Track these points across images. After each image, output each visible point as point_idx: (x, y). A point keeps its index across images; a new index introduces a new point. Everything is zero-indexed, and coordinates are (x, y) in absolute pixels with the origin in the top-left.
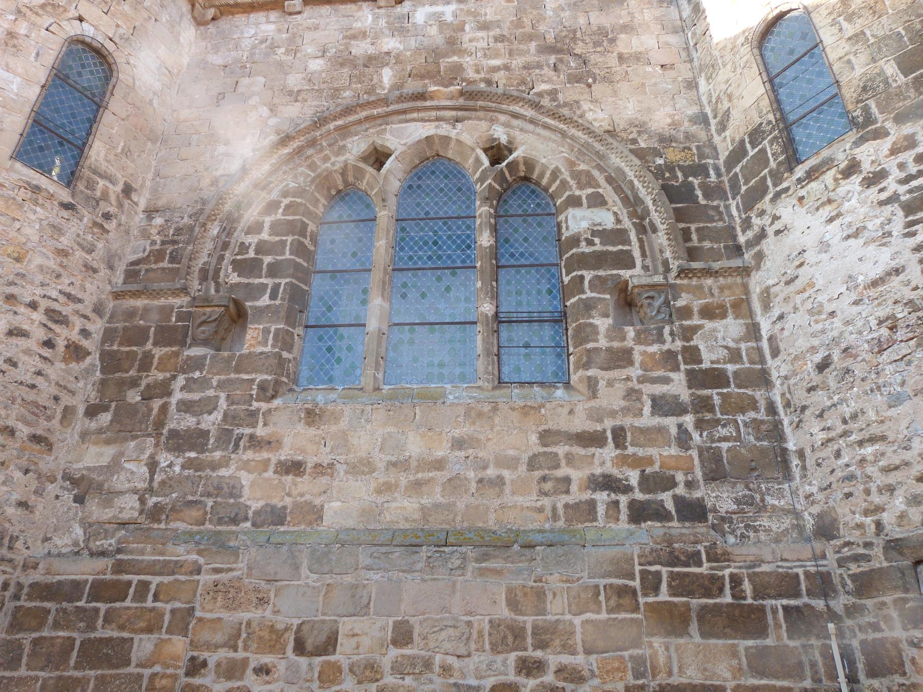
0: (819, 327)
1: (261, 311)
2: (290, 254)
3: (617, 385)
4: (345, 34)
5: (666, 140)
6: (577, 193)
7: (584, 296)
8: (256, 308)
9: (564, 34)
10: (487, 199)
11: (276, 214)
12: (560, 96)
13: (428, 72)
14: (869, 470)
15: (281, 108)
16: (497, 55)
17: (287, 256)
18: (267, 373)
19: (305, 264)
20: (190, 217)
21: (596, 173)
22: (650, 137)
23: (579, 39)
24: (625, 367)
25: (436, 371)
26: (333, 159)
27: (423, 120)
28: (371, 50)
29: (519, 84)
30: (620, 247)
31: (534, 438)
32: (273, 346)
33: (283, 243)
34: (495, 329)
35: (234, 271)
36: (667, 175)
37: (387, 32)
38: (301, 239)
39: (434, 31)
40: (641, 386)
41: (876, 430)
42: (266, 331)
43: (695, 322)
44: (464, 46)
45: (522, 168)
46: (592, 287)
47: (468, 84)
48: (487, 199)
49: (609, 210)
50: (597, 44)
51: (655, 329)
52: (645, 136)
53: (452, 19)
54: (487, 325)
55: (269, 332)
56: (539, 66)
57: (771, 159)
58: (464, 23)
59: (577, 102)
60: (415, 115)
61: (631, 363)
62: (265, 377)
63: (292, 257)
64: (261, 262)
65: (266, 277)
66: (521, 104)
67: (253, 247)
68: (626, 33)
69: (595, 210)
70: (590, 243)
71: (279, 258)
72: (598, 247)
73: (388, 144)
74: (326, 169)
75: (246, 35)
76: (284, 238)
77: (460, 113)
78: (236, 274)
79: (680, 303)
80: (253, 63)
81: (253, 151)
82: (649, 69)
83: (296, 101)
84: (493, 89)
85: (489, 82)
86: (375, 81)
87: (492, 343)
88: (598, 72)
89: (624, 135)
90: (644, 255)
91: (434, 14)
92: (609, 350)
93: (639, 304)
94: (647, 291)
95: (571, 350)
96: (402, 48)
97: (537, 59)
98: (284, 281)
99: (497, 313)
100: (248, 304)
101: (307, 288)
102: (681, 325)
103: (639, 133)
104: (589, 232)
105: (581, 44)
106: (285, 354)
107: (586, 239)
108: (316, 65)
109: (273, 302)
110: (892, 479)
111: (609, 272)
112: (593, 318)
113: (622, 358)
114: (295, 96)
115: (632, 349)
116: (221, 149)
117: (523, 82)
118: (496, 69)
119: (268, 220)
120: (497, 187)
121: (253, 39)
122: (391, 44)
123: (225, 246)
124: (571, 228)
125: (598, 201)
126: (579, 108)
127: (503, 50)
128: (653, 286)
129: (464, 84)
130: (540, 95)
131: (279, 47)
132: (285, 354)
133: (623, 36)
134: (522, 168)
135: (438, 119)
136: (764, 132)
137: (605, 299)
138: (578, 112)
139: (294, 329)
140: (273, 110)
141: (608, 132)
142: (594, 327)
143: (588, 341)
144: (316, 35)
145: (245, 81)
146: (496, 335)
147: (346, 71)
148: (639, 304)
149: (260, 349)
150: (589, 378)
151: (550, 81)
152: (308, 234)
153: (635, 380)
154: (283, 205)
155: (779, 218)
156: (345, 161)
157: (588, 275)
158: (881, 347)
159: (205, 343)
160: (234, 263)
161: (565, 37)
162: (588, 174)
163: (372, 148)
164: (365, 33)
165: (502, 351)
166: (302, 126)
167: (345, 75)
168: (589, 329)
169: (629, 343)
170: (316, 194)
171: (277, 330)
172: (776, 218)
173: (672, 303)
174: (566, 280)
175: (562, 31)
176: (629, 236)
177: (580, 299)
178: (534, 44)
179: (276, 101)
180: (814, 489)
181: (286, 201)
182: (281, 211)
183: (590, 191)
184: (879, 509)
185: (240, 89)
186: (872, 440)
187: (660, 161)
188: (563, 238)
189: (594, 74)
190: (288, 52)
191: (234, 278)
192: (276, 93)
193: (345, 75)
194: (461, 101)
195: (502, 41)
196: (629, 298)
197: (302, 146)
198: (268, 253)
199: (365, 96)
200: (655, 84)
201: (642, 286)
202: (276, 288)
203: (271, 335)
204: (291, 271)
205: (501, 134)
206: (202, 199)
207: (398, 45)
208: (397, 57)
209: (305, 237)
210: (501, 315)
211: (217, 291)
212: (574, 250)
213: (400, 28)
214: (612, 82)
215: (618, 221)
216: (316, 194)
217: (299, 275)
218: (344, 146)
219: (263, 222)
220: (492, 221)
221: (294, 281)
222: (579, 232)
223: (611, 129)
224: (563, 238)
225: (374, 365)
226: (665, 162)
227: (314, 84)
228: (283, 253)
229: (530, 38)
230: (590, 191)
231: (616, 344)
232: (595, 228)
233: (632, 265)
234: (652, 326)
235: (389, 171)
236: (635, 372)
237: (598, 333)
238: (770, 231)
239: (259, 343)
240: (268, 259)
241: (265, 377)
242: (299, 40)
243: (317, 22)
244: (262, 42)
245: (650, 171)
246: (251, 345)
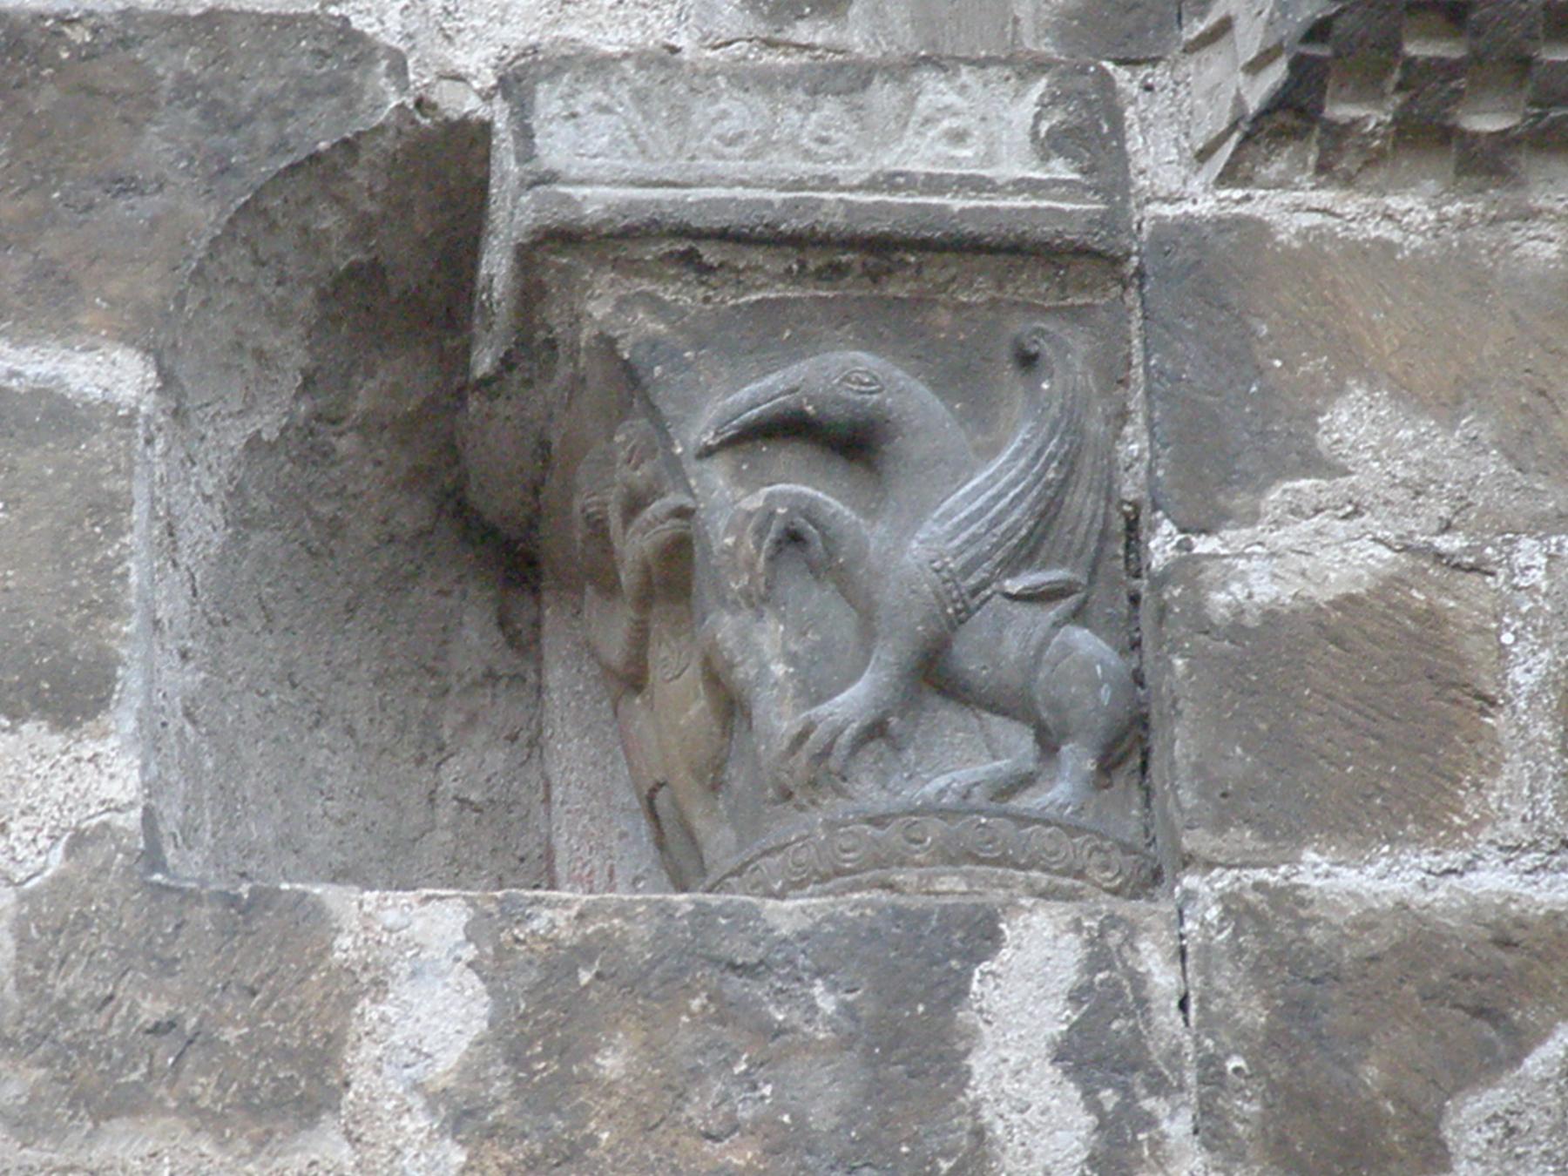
43: (1493, 880)
79: (1279, 558)
93: (635, 546)
102: (1267, 922)
128: (874, 262)
137: (58, 415)
148: (635, 546)
173: (1162, 544)
196: (494, 440)
201: (691, 246)
234: (787, 914)
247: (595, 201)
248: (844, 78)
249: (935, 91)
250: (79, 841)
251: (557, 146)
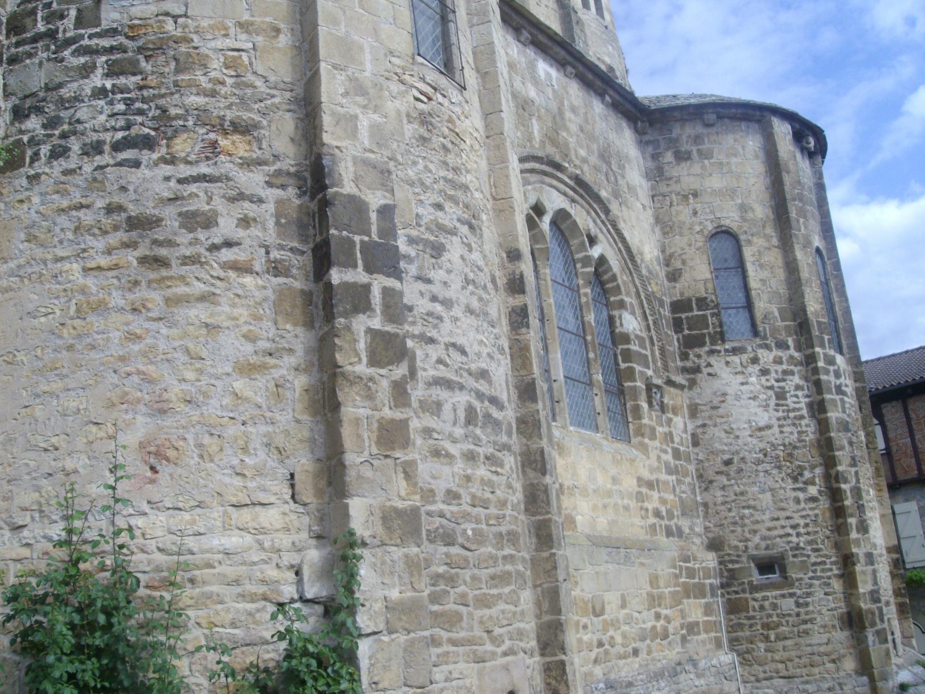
0: (729, 441)
14: (746, 521)
31: (635, 481)
41: (752, 503)
57: (711, 326)
60: (555, 183)
110: (756, 527)
136: (708, 305)
155: (711, 366)
158: (758, 462)
172: (709, 365)
180: (711, 525)
184: (747, 540)
186: (749, 507)
238: (705, 371)
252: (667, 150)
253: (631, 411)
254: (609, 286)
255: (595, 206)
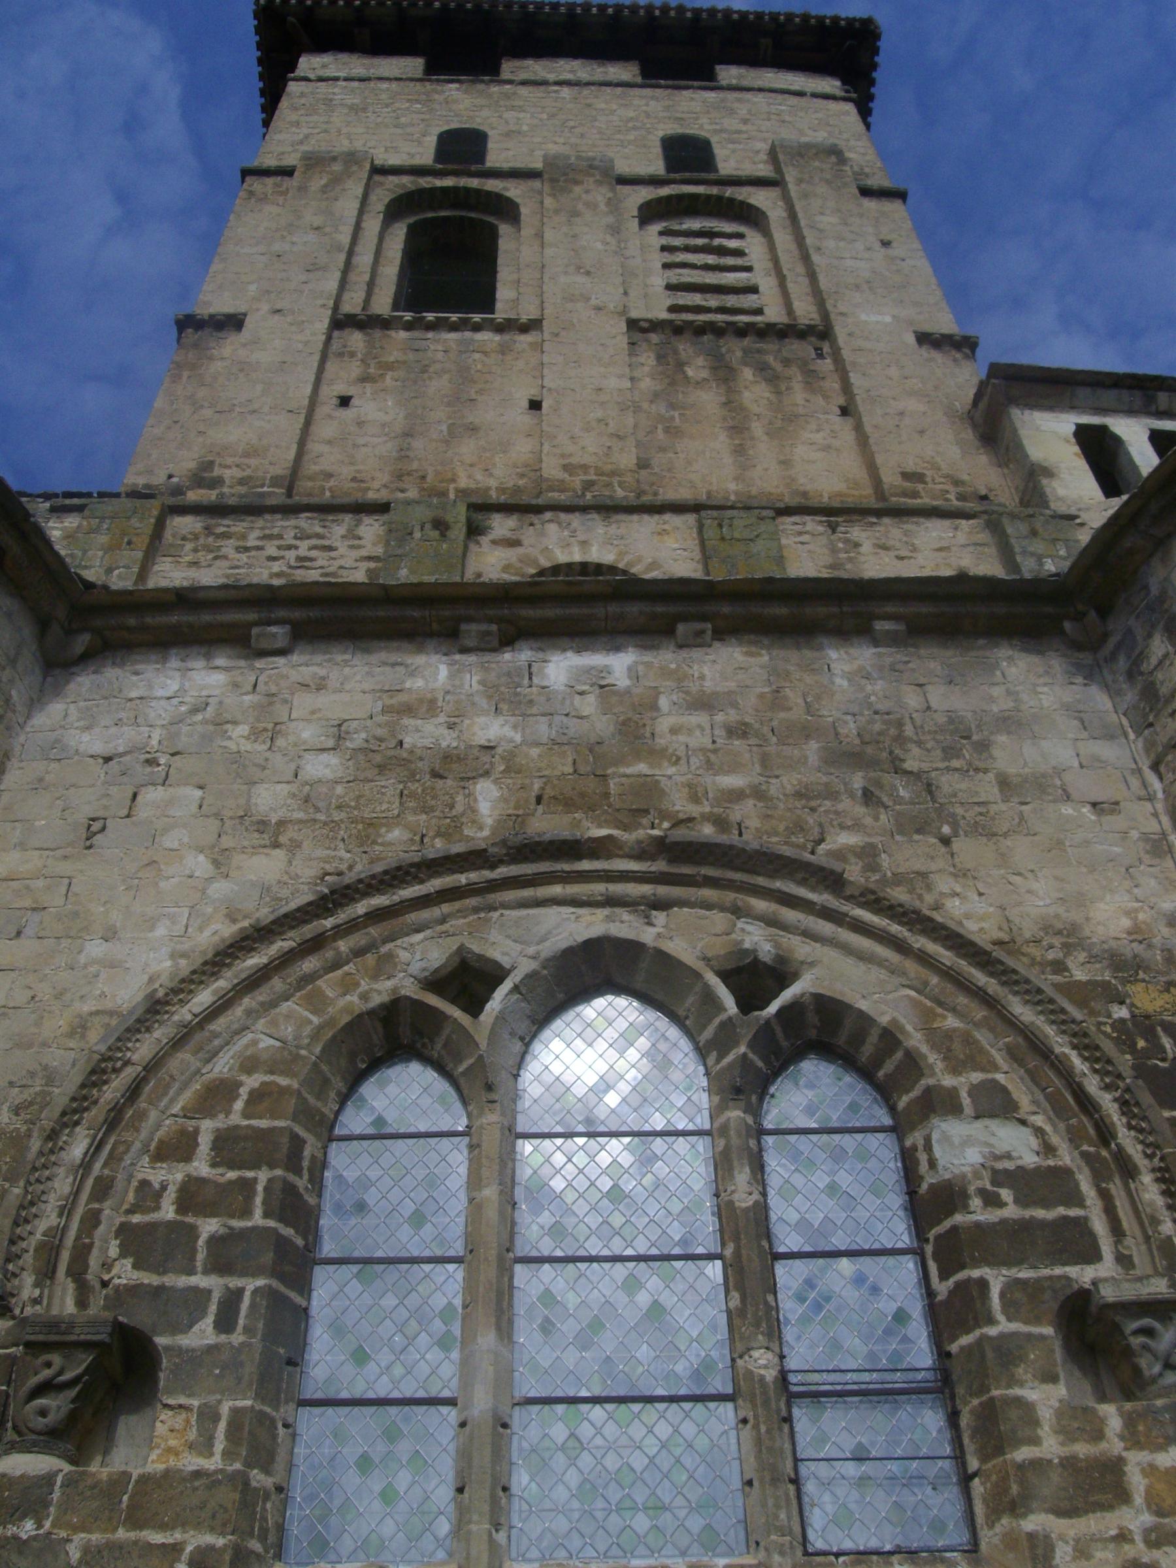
1: (194, 1360)
2: (266, 1215)
3: (1099, 1555)
4: (389, 702)
5: (1126, 967)
6: (948, 1081)
7: (992, 1331)
8: (180, 1351)
9: (877, 727)
10: (738, 1091)
11: (228, 1113)
12: (884, 860)
13: (582, 795)
15: (237, 859)
16: (734, 767)
17: (258, 1218)
18: (212, 1529)
19: (300, 1242)
20: (16, 1111)
21: (982, 1037)
22: (1093, 958)
23: (911, 740)
24: (1111, 1507)
25: (641, 1523)
26: (364, 985)
27: (575, 902)
28: (448, 739)
29: (790, 831)
30: (1061, 1211)
32: (227, 1454)
33: (247, 1186)
34: (784, 1413)
35: (123, 1255)
36: (1141, 1044)
37: (483, 703)
38: (292, 1178)
39: (589, 705)
40: (1157, 1554)
42: (208, 1416)
44: (661, 742)
45: (812, 1018)
46: (1011, 1308)
47: (673, 826)
48: (738, 1091)
49: (1023, 1122)
50: (950, 752)
51: (1166, 1408)
52: (1082, 956)
53: (627, 682)
54: (766, 1403)
55: (216, 1418)
56: (831, 794)
58: (656, 692)
59: (924, 875)
60: (557, 890)
61: (1123, 1496)
62: (209, 1539)
63: (272, 1223)
64: (192, 1232)
65: (206, 1272)
66: (799, 876)
67: (170, 1195)
68: (1009, 733)
69: (994, 1124)
70: (992, 1201)
71: (237, 1224)
72: (1011, 1212)
73: (495, 954)
74: (346, 1010)
75: (160, 693)
76: (250, 1174)
77: (663, 890)
78: (128, 1263)
80: (173, 755)
81: (173, 956)
82: (1067, 810)
83: (276, 845)
84: (732, 838)
85: (721, 823)
86: (459, 808)
87: (782, 1451)
88: (959, 811)
89: (1032, 950)
90: (1117, 1231)
91: (589, 670)
92: (1069, 1463)
94: (1138, 1316)
95: (973, 1464)
96: (518, 738)
97: (825, 779)
98: (252, 1284)
99: (783, 1375)
100: (161, 1341)
101: (304, 1304)
103: (1068, 948)
104: (986, 1175)
105: (916, 750)
106: (257, 1478)
107: (982, 1192)
108: (322, 767)
109: (223, 1338)
111: (1046, 1272)
112: (1021, 1384)
113: (1099, 1485)
114: (271, 833)
115: (1120, 1461)
116: (95, 949)
117: (799, 827)
118: (736, 796)
119: (207, 1128)
120: (760, 1064)
121: (175, 701)
122: (491, 728)
123: (103, 1189)
124: (941, 1162)
125: (996, 1104)
126: (929, 888)
127: (747, 756)
129: (666, 825)
130: (840, 855)
131: (235, 723)
132: (257, 1478)
133: (1002, 738)
134: (812, 1018)
135: (611, 902)
137: (1042, 1338)
138: (929, 899)
139: (276, 1408)
140: (220, 861)
141: (999, 943)
142: (1027, 1409)
143: (1018, 1443)
144: (322, 700)
145: (152, 795)
146: (786, 1428)
147: (390, 785)
149: (192, 1462)
150: (1031, 1536)
151: (857, 826)
152: (306, 1164)
153: (1138, 1538)
154: (244, 1092)
156: (395, 990)
157: (996, 1279)
159: (52, 1438)
160: (124, 1231)
161: (879, 734)
162: (968, 1040)
163: (457, 959)
164: (432, 702)
165: (804, 1469)
166: (293, 906)
167: (390, 792)
168: (1014, 1414)
169: (1114, 1445)
170: (325, 1068)
171: (236, 1412)
174: (942, 1289)
175: (871, 722)
176: (1077, 1185)
177: (984, 1338)
178: (814, 745)
179: (226, 842)
181: (252, 1082)
182: (239, 1105)
183: (976, 1077)
185: (143, 812)
187: (1122, 1013)
188: (925, 1186)
189: (953, 815)
190: (255, 734)
191: (125, 1273)
192: (228, 823)
193: (390, 792)
194: (660, 866)
195: (744, 735)
197: (291, 950)
198: (208, 1210)
199: (438, 843)
200: (1087, 843)
202: (232, 1300)
203: (222, 1426)
204: (268, 1257)
205: (756, 939)
206: (45, 1068)
207: (508, 732)
208: (510, 758)
209: (298, 1171)
210: (793, 1378)
211: (82, 1303)
212: (958, 1218)
213: (511, 699)
214: (994, 835)
215: (1048, 1149)
216: (325, 1068)
217: (288, 1268)
218: (390, 956)
219: (197, 1131)
220: (752, 1143)
221: (275, 1283)
222: (964, 1176)
223: (1006, 938)
224: (925, 1186)
225: (486, 1508)
226: (1133, 1016)
227: (317, 809)
228: (246, 1212)
229: (807, 732)
230: (976, 1077)
231: (1082, 1449)
232: (1000, 1165)
233: (1092, 1255)
235: (501, 1018)
236: (1135, 1518)
237: (1036, 1423)
239: (191, 1446)
240: (209, 1227)
241: (209, 1539)
242: (281, 712)
243: (322, 672)
244: (195, 710)
245: (1104, 1033)
246: (169, 1450)
247: (1111, 1300)
248: (1140, 1279)
249: (1153, 1280)
250: (1060, 1401)
251: (1103, 1292)
252: (1150, 636)
253: (972, 1437)
254: (889, 1067)
255: (778, 884)
